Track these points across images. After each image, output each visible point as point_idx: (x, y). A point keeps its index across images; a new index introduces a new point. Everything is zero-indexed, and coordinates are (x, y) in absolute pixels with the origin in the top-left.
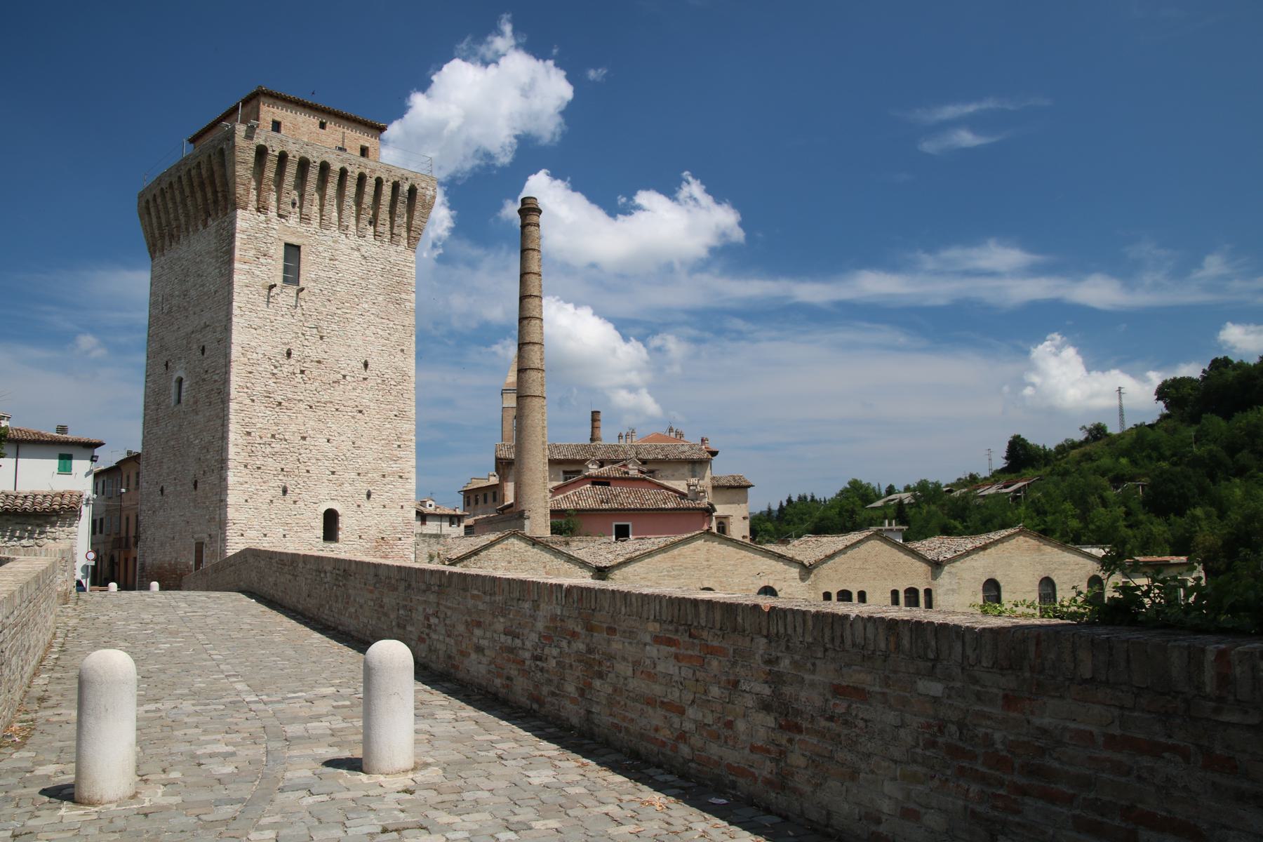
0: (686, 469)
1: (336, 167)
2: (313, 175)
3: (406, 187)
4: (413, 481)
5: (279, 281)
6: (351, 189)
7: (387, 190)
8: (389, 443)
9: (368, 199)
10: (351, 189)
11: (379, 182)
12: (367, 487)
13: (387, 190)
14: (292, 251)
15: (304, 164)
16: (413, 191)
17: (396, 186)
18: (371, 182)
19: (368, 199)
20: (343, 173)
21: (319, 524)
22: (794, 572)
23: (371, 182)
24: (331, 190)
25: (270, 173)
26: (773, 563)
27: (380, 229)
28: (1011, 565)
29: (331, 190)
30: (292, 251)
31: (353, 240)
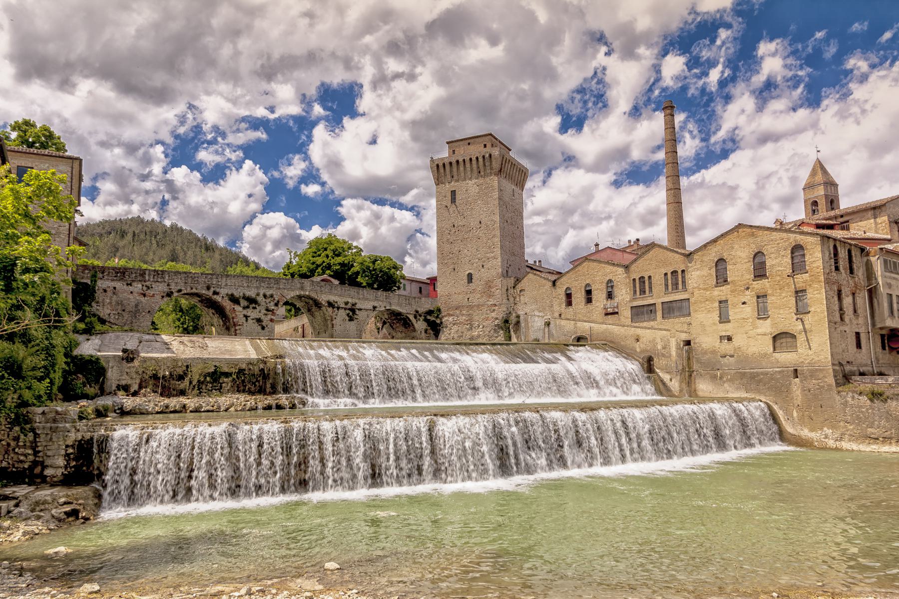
0: (870, 213)
1: (461, 160)
2: (454, 165)
3: (487, 155)
4: (500, 259)
5: (449, 204)
6: (468, 165)
7: (481, 160)
8: (490, 247)
9: (475, 166)
10: (468, 165)
11: (477, 158)
12: (480, 264)
13: (481, 160)
14: (453, 193)
15: (451, 163)
16: (490, 156)
17: (484, 157)
18: (474, 159)
19: (475, 166)
20: (464, 160)
21: (466, 277)
22: (621, 270)
23: (474, 159)
24: (462, 168)
25: (442, 170)
26: (611, 267)
27: (482, 173)
28: (733, 248)
29: (462, 168)
30: (453, 193)
31: (474, 181)
